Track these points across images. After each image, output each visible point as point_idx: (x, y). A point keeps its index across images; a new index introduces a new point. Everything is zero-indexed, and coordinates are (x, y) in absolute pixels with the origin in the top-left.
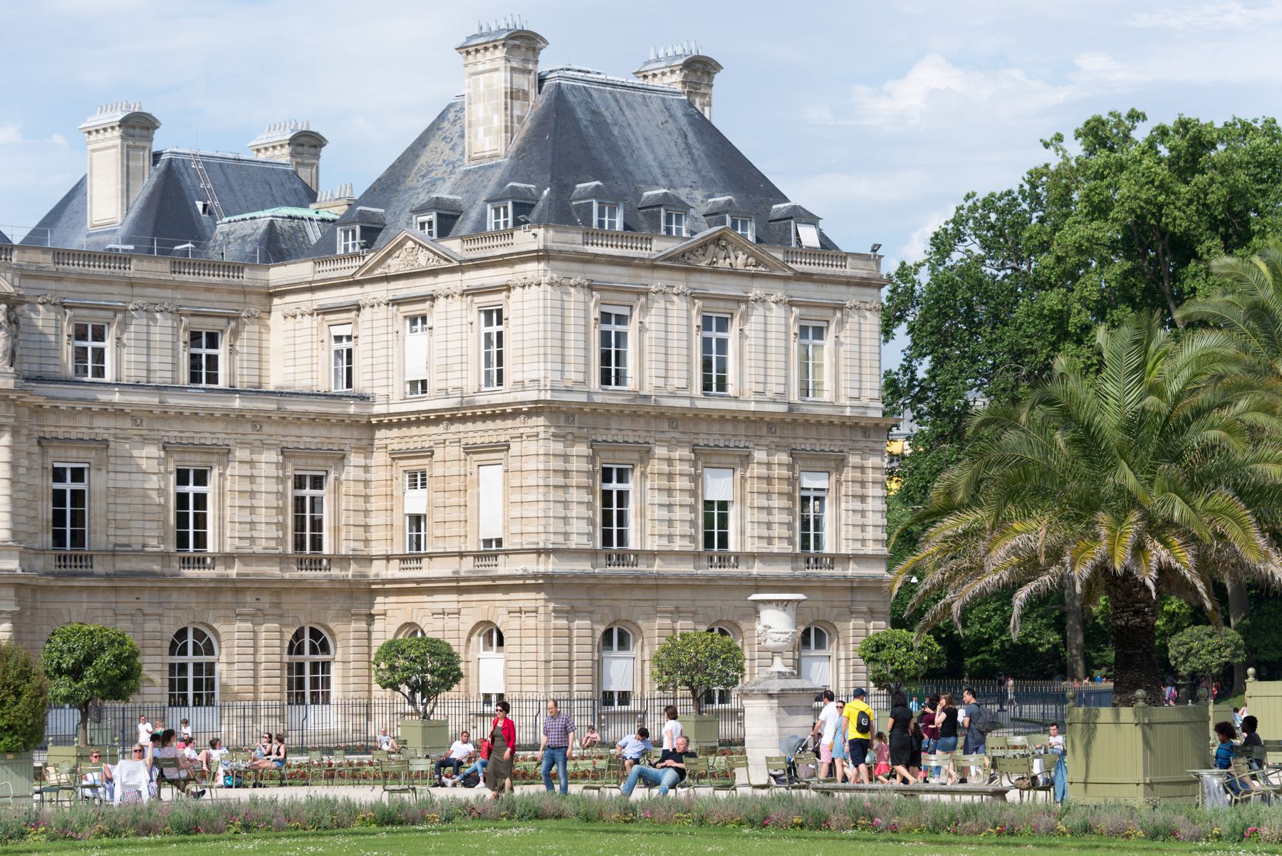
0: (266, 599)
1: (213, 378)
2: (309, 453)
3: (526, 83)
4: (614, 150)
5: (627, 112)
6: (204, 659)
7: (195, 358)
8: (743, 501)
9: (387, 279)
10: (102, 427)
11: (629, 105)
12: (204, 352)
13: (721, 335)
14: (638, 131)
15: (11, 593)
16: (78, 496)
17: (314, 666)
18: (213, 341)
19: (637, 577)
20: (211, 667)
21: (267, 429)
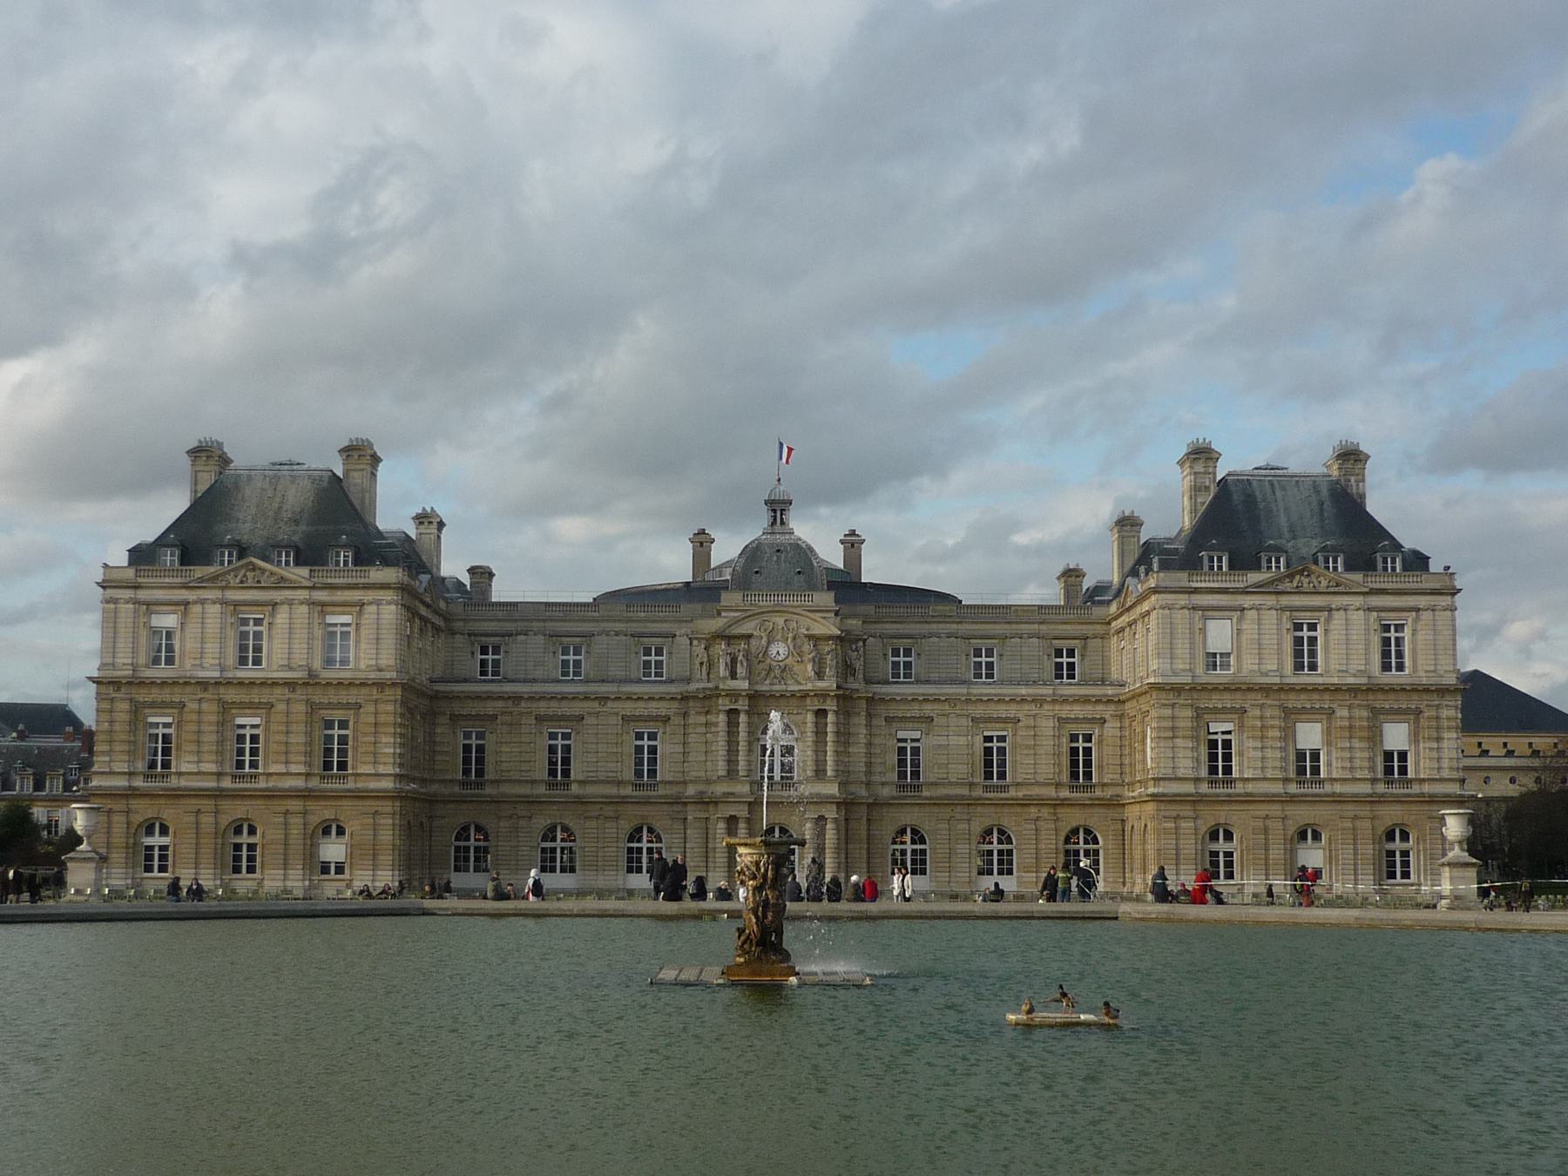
0: (1045, 812)
2: (1076, 720)
5: (1279, 493)
6: (1005, 847)
7: (1059, 666)
8: (1329, 744)
9: (1128, 610)
10: (928, 709)
11: (1284, 489)
12: (1065, 660)
13: (1312, 634)
15: (834, 807)
16: (916, 751)
18: (1071, 653)
19: (1229, 795)
21: (1046, 707)
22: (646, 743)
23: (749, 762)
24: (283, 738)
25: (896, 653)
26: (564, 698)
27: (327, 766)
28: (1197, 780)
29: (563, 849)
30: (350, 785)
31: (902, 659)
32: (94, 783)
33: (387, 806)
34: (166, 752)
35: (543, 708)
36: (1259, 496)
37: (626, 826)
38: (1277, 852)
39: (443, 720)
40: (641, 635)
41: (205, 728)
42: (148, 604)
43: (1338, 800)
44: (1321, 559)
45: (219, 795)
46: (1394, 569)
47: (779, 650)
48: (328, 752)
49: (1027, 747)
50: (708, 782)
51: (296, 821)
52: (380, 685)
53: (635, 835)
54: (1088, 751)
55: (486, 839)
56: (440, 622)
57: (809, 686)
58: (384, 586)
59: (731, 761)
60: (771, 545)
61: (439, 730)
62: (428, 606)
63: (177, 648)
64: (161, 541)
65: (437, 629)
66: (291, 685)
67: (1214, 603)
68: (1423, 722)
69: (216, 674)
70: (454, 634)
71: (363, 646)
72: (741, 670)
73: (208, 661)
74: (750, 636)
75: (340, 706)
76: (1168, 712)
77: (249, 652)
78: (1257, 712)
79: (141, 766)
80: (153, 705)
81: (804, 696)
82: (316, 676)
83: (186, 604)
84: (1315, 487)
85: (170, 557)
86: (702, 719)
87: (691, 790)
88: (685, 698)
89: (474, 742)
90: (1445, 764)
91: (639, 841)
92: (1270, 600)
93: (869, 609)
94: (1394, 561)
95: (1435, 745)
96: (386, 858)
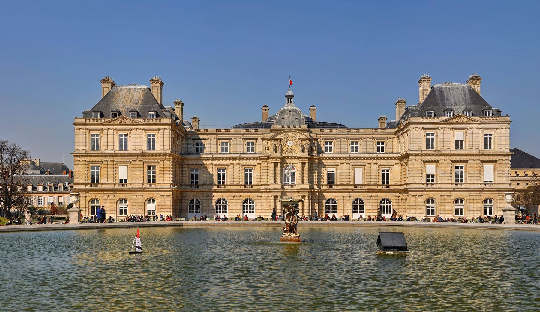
0: (374, 194)
1: (383, 151)
2: (384, 165)
3: (428, 87)
4: (443, 99)
5: (451, 91)
6: (361, 204)
7: (378, 148)
11: (453, 89)
14: (452, 95)
16: (333, 175)
17: (387, 206)
18: (383, 143)
20: (363, 206)
21: (375, 161)
22: (249, 173)
23: (281, 179)
24: (134, 172)
26: (223, 159)
27: (149, 181)
28: (423, 184)
29: (223, 206)
30: (157, 186)
32: (74, 187)
33: (168, 193)
34: (98, 177)
36: (445, 92)
37: (243, 199)
38: (448, 207)
40: (246, 139)
41: (109, 169)
42: (90, 130)
43: (469, 190)
44: (465, 112)
45: (115, 191)
46: (489, 115)
47: (290, 143)
48: (149, 176)
49: (368, 173)
50: (269, 185)
52: (165, 155)
53: (245, 201)
54: (388, 175)
55: (199, 203)
56: (183, 135)
57: (300, 155)
58: (166, 124)
59: (275, 178)
60: (287, 110)
61: (184, 169)
62: (180, 130)
63: (100, 144)
64: (93, 110)
65: (183, 138)
66: (136, 155)
67: (429, 127)
68: (497, 165)
69: (113, 152)
70: (187, 139)
71: (159, 143)
72: (278, 150)
73: (109, 149)
74: (281, 139)
75: (153, 162)
76: (414, 162)
77: (123, 145)
78: (443, 162)
79: (89, 181)
80: (92, 162)
81: (298, 158)
82: (145, 153)
83: (102, 130)
84: (464, 89)
85: (97, 115)
86: (266, 165)
87: (263, 187)
88: (261, 159)
90: (505, 178)
91: (247, 203)
92: (448, 126)
93: (318, 131)
94: (489, 113)
95: (501, 172)
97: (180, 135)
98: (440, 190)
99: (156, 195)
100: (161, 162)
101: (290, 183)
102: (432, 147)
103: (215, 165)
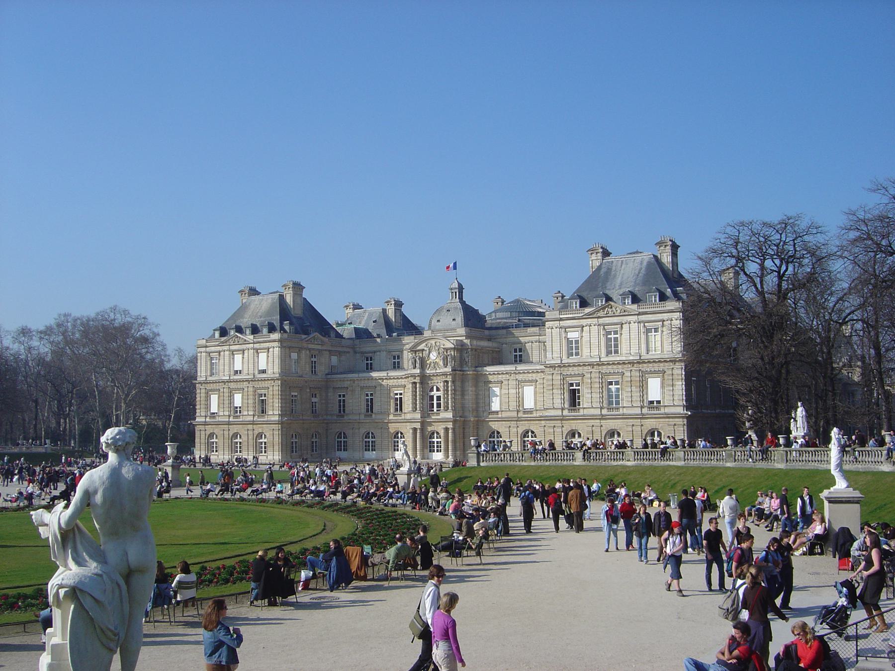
25: (515, 351)
31: (518, 354)
33: (276, 427)
35: (362, 384)
36: (614, 268)
39: (331, 390)
47: (433, 356)
51: (250, 433)
56: (348, 350)
57: (442, 370)
58: (274, 341)
70: (355, 352)
83: (219, 352)
85: (217, 334)
89: (342, 398)
96: (276, 447)
97: (320, 351)
98: (585, 418)
99: (267, 430)
100: (271, 389)
101: (435, 409)
102: (577, 354)
103: (362, 388)
